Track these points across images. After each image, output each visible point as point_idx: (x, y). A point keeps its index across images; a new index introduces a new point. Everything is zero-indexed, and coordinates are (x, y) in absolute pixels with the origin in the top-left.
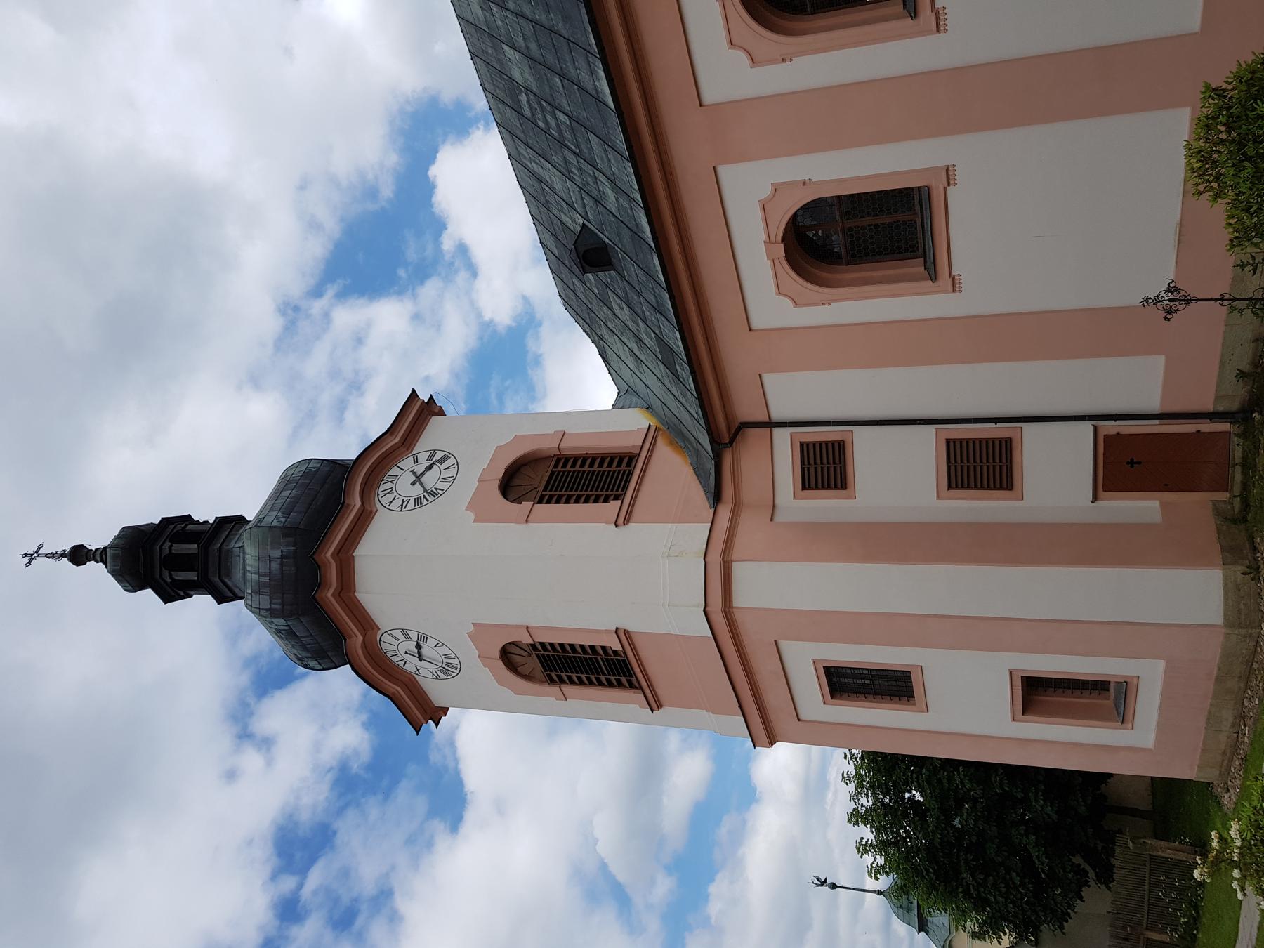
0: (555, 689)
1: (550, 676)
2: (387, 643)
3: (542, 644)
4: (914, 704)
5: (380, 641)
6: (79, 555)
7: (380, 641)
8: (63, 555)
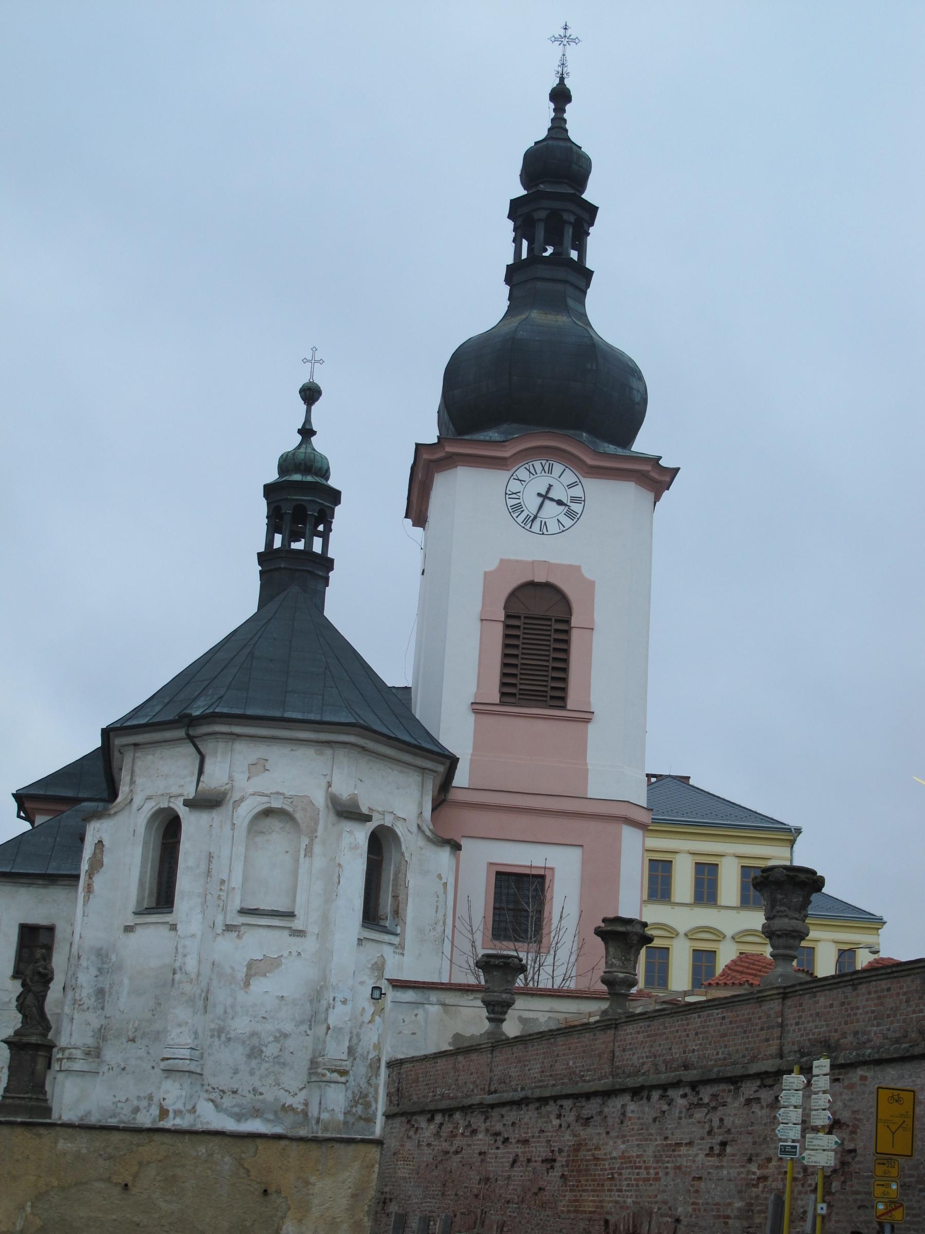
5: (566, 467)
7: (566, 467)
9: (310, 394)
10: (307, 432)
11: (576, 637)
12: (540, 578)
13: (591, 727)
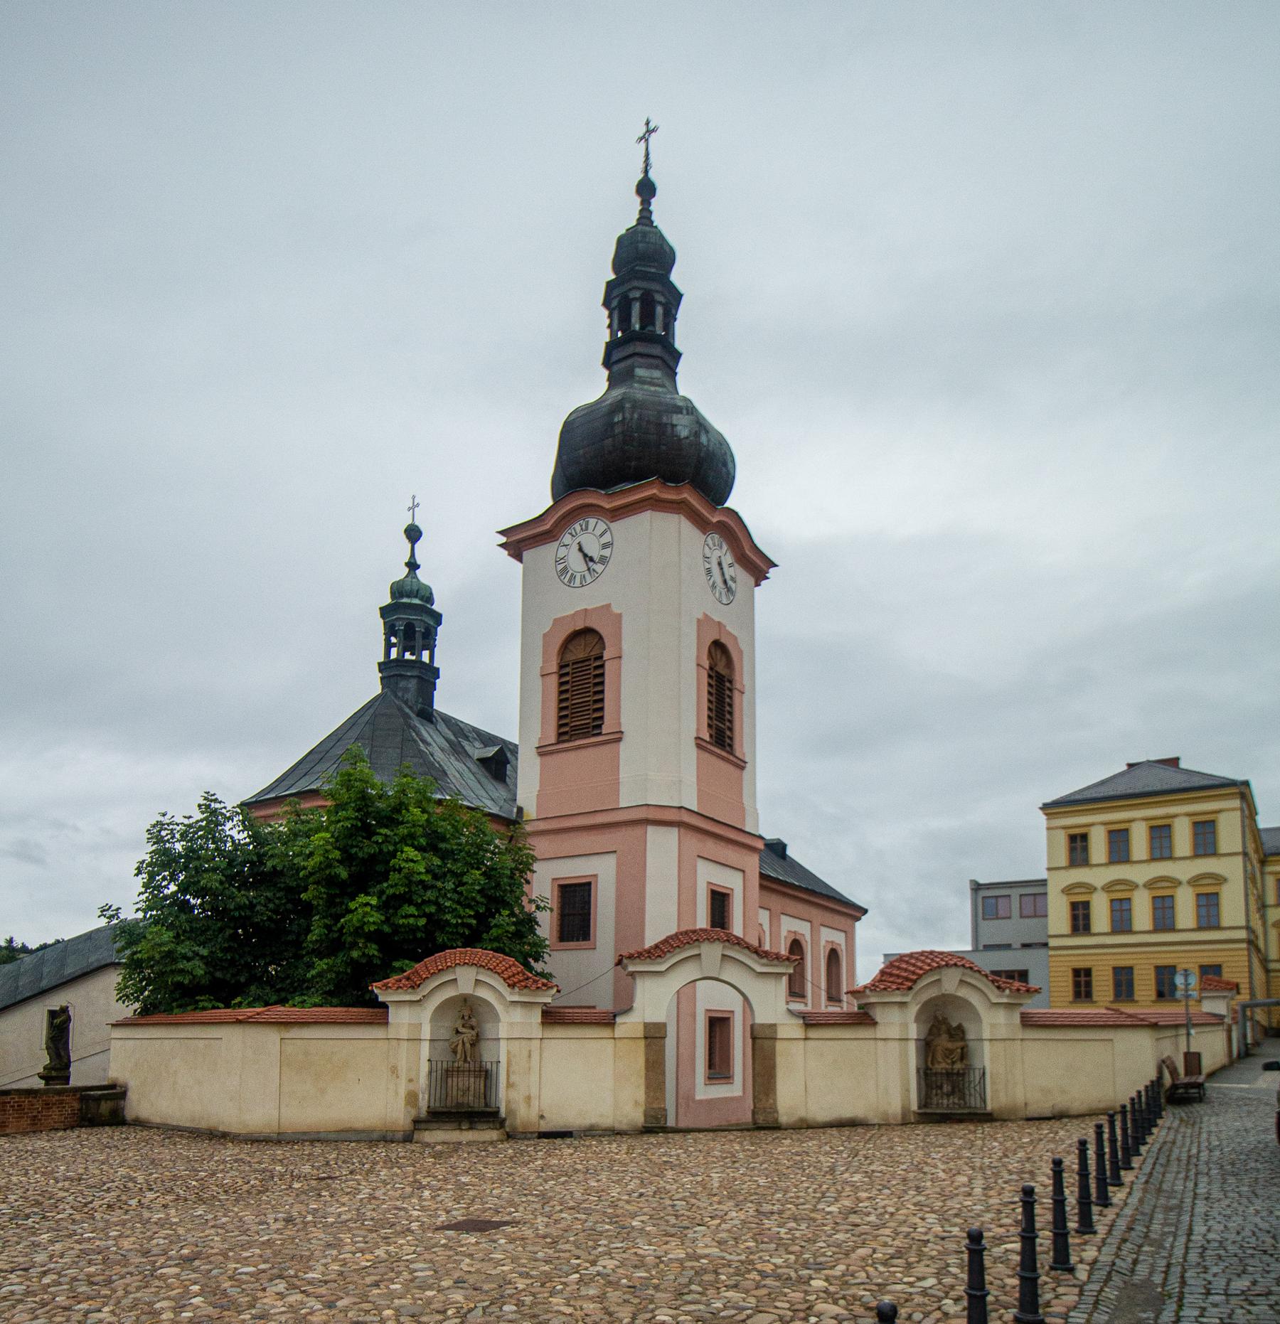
0: (553, 667)
1: (568, 665)
2: (596, 524)
3: (602, 666)
4: (886, 956)
6: (646, 189)
8: (646, 172)
9: (413, 534)
10: (413, 566)
11: (609, 668)
12: (580, 626)
13: (622, 744)
